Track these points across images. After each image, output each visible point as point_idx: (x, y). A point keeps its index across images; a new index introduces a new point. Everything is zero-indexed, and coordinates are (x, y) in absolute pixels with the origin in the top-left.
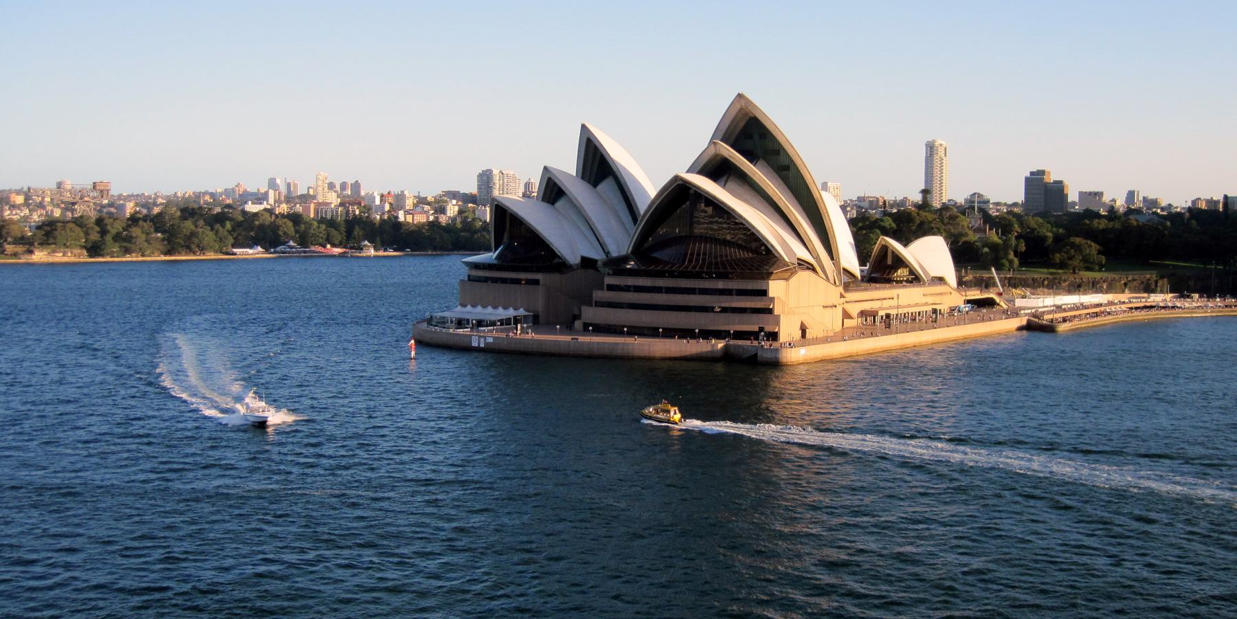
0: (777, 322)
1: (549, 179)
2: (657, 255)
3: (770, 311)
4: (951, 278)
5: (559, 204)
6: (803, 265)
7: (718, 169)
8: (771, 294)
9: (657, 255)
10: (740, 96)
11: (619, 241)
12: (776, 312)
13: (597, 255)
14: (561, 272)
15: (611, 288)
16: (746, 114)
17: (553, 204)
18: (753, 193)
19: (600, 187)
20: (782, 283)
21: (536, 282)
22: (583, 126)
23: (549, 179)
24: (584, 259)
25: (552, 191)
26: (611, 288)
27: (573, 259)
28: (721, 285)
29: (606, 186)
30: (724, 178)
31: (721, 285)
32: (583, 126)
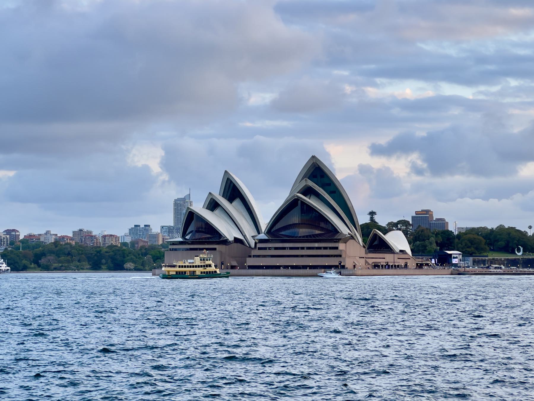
3: (340, 256)
4: (409, 252)
5: (217, 211)
10: (313, 157)
12: (343, 256)
13: (240, 237)
14: (226, 244)
19: (234, 203)
20: (344, 244)
21: (215, 249)
22: (226, 172)
24: (235, 238)
25: (213, 205)
27: (231, 239)
30: (309, 196)
31: (316, 245)
32: (226, 172)
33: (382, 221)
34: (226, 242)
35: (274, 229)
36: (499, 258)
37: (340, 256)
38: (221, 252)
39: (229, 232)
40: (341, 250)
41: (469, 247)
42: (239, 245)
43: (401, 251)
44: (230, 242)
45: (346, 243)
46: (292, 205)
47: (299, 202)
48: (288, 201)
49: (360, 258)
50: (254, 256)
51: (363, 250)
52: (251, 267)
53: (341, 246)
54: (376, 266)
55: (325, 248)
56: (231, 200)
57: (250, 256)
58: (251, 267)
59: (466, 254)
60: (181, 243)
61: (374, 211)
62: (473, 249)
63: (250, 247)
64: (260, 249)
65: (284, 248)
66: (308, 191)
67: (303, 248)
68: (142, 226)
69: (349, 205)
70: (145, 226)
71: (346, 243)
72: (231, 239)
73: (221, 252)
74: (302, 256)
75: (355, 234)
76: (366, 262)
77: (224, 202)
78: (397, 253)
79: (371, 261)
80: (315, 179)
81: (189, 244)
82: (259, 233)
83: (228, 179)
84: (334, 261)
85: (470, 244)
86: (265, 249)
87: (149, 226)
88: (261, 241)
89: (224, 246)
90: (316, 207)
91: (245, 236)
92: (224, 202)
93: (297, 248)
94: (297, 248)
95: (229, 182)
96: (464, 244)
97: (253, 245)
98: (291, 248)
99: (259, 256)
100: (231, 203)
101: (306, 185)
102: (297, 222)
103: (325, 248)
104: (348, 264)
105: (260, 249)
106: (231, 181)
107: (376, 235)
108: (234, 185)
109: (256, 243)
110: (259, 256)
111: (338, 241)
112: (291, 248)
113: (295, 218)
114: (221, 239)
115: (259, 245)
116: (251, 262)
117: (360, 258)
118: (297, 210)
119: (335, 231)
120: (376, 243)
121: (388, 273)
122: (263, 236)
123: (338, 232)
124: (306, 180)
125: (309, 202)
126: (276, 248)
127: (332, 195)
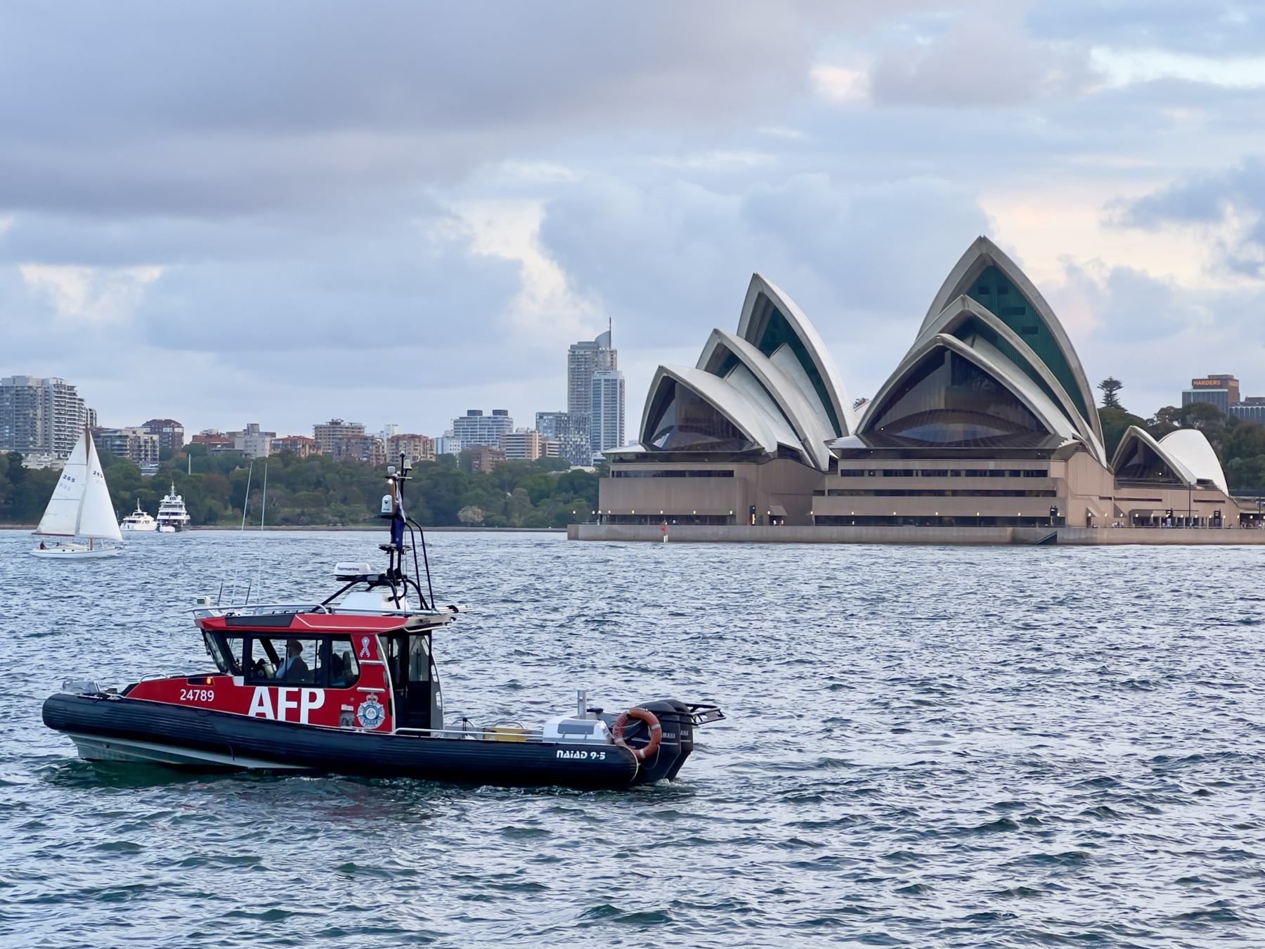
3: (1053, 494)
5: (734, 378)
9: (903, 434)
10: (982, 241)
21: (730, 474)
22: (756, 277)
24: (780, 446)
25: (723, 361)
27: (770, 448)
28: (991, 465)
30: (970, 340)
31: (991, 465)
32: (756, 277)
33: (1141, 403)
34: (756, 455)
35: (880, 425)
37: (1053, 494)
38: (745, 482)
39: (765, 431)
40: (1055, 479)
42: (791, 462)
43: (1200, 482)
44: (767, 455)
45: (1066, 460)
47: (948, 355)
48: (920, 351)
49: (1101, 498)
51: (1110, 479)
52: (821, 520)
53: (1056, 469)
54: (1143, 521)
55: (1015, 473)
56: (767, 348)
57: (822, 493)
58: (821, 520)
60: (640, 457)
61: (1115, 379)
63: (818, 468)
64: (846, 473)
66: (968, 327)
67: (956, 473)
68: (487, 413)
69: (1073, 364)
70: (495, 412)
71: (1066, 460)
72: (770, 448)
73: (745, 482)
74: (955, 493)
75: (1089, 439)
76: (1117, 512)
77: (749, 353)
78: (1190, 488)
79: (1126, 507)
80: (983, 297)
82: (839, 435)
83: (761, 295)
84: (1039, 508)
86: (860, 473)
87: (505, 413)
88: (849, 454)
89: (753, 466)
90: (990, 369)
91: (804, 442)
92: (749, 353)
93: (943, 473)
94: (943, 473)
95: (763, 303)
97: (825, 465)
98: (926, 473)
99: (841, 493)
100: (768, 356)
101: (962, 313)
102: (943, 407)
103: (1015, 473)
104: (1074, 515)
105: (846, 473)
106: (769, 302)
107: (1136, 442)
108: (776, 310)
109: (833, 461)
110: (841, 493)
111: (1046, 455)
112: (926, 473)
113: (934, 394)
114: (745, 449)
115: (843, 465)
116: (822, 506)
117: (1101, 498)
118: (942, 375)
119: (1040, 428)
120: (1135, 460)
121: (1175, 538)
122: (851, 440)
123: (1047, 433)
124: (963, 300)
125: (973, 356)
126: (888, 473)
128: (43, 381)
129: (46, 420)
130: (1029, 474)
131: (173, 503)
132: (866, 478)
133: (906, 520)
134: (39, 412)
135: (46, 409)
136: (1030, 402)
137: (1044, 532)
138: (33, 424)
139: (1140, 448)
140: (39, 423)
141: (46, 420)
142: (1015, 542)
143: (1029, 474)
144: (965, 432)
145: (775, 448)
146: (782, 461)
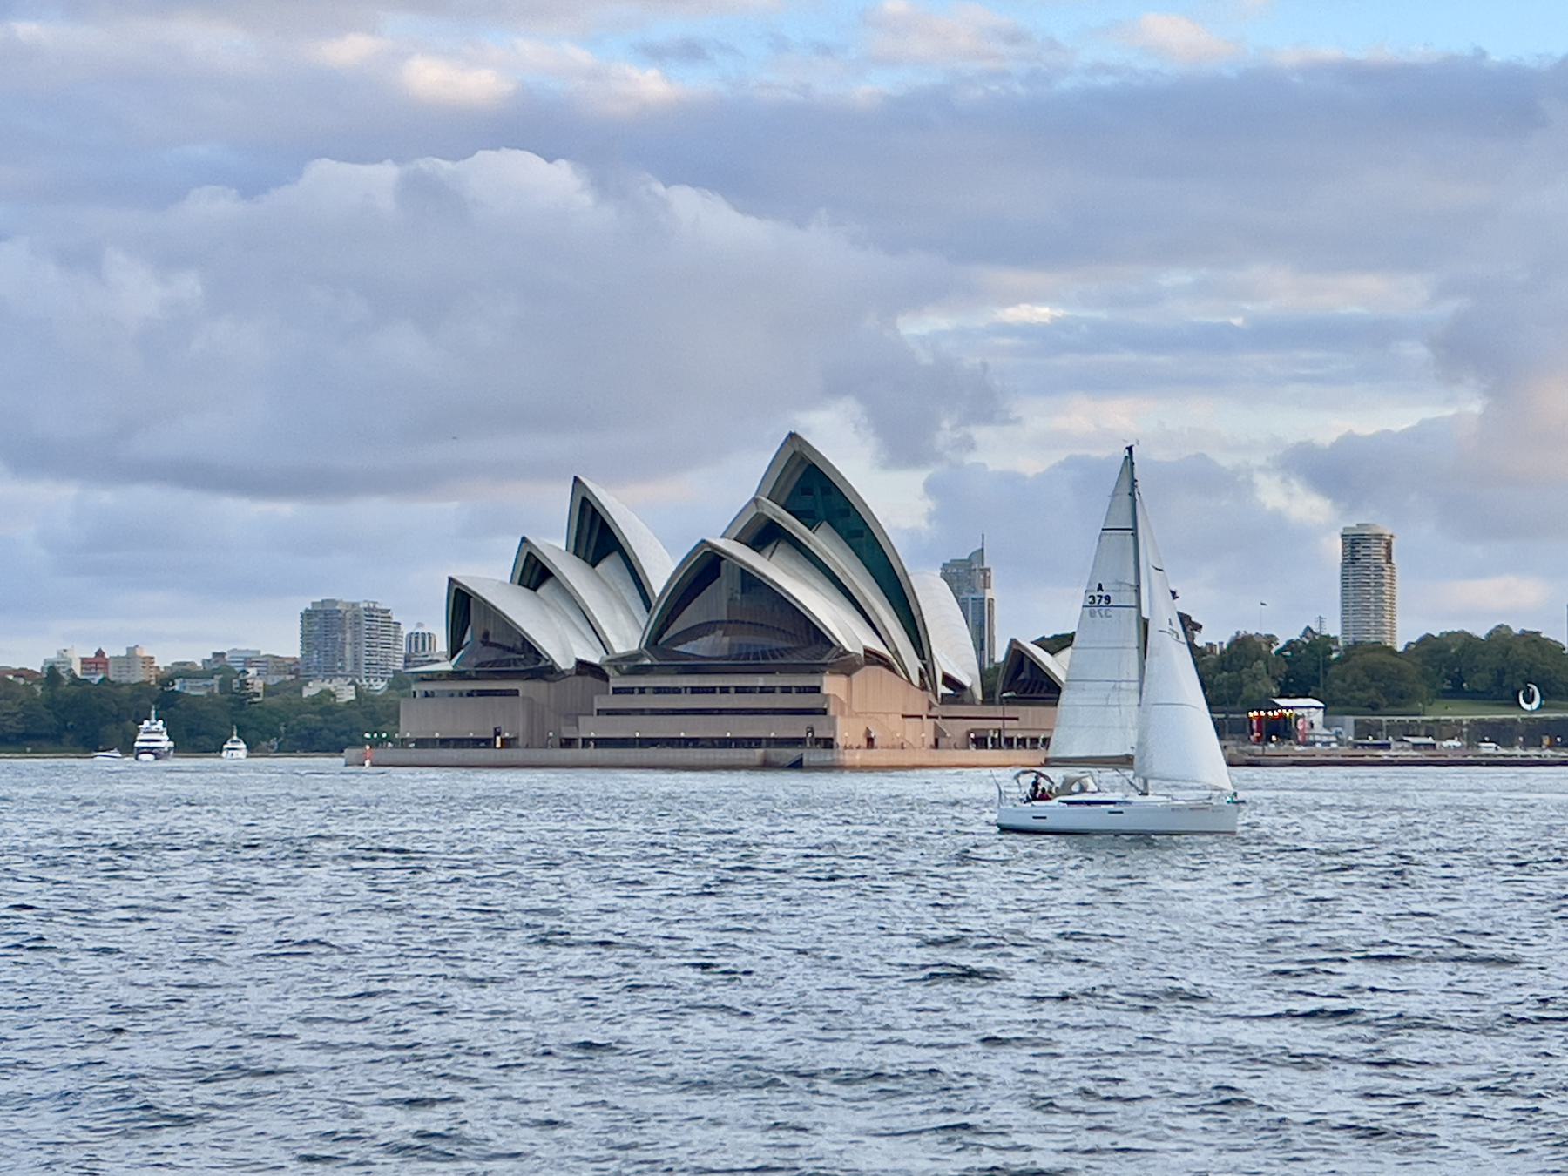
0: (833, 727)
1: (529, 554)
2: (680, 648)
3: (824, 712)
5: (544, 590)
6: (872, 657)
7: (763, 535)
8: (825, 690)
9: (680, 648)
10: (792, 436)
11: (625, 633)
12: (831, 712)
15: (616, 691)
16: (804, 460)
17: (535, 589)
18: (794, 552)
19: (599, 567)
20: (843, 679)
21: (516, 693)
22: (576, 479)
23: (529, 554)
24: (580, 663)
25: (534, 573)
26: (616, 691)
27: (565, 663)
28: (761, 681)
29: (610, 565)
30: (771, 547)
31: (761, 681)
32: (576, 479)
35: (665, 637)
36: (1453, 718)
38: (530, 701)
39: (563, 645)
41: (1365, 688)
44: (562, 672)
46: (705, 568)
50: (599, 712)
53: (832, 685)
55: (786, 690)
59: (1332, 706)
60: (454, 675)
62: (1373, 692)
65: (677, 691)
67: (725, 690)
81: (470, 679)
83: (584, 500)
85: (1367, 680)
86: (630, 691)
89: (544, 684)
93: (712, 690)
94: (712, 690)
96: (1349, 680)
98: (695, 690)
100: (594, 565)
103: (786, 690)
104: (846, 731)
111: (817, 670)
112: (695, 690)
113: (715, 602)
114: (542, 664)
116: (591, 727)
121: (982, 761)
123: (832, 645)
127: (855, 541)
128: (353, 605)
129: (356, 644)
130: (802, 690)
131: (153, 731)
132: (636, 697)
133: (724, 743)
134: (348, 636)
135: (356, 634)
136: (873, 609)
137: (792, 754)
138: (343, 652)
139: (1026, 663)
140: (348, 648)
141: (356, 644)
142: (767, 766)
143: (802, 690)
144: (731, 645)
145: (572, 665)
146: (579, 678)
